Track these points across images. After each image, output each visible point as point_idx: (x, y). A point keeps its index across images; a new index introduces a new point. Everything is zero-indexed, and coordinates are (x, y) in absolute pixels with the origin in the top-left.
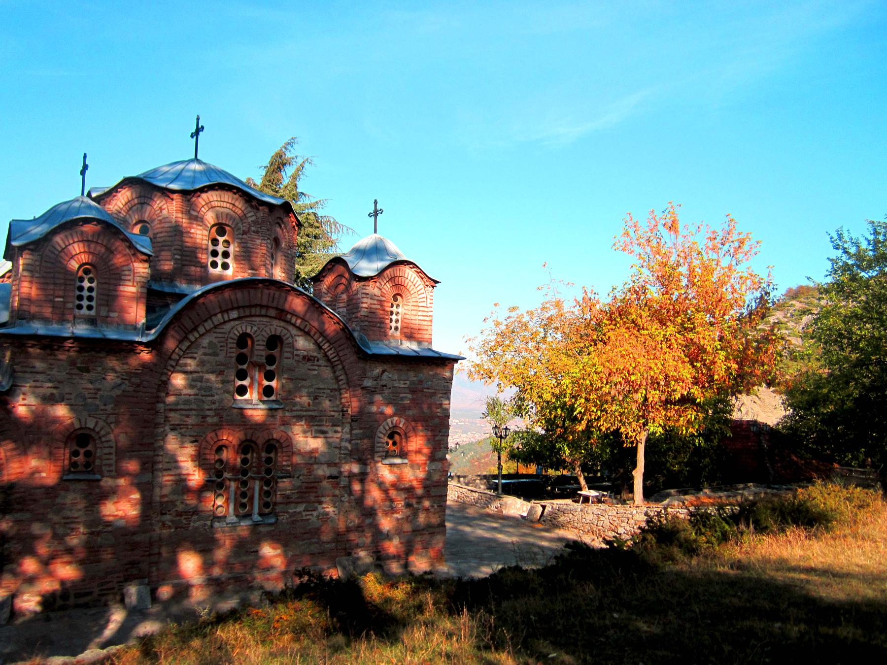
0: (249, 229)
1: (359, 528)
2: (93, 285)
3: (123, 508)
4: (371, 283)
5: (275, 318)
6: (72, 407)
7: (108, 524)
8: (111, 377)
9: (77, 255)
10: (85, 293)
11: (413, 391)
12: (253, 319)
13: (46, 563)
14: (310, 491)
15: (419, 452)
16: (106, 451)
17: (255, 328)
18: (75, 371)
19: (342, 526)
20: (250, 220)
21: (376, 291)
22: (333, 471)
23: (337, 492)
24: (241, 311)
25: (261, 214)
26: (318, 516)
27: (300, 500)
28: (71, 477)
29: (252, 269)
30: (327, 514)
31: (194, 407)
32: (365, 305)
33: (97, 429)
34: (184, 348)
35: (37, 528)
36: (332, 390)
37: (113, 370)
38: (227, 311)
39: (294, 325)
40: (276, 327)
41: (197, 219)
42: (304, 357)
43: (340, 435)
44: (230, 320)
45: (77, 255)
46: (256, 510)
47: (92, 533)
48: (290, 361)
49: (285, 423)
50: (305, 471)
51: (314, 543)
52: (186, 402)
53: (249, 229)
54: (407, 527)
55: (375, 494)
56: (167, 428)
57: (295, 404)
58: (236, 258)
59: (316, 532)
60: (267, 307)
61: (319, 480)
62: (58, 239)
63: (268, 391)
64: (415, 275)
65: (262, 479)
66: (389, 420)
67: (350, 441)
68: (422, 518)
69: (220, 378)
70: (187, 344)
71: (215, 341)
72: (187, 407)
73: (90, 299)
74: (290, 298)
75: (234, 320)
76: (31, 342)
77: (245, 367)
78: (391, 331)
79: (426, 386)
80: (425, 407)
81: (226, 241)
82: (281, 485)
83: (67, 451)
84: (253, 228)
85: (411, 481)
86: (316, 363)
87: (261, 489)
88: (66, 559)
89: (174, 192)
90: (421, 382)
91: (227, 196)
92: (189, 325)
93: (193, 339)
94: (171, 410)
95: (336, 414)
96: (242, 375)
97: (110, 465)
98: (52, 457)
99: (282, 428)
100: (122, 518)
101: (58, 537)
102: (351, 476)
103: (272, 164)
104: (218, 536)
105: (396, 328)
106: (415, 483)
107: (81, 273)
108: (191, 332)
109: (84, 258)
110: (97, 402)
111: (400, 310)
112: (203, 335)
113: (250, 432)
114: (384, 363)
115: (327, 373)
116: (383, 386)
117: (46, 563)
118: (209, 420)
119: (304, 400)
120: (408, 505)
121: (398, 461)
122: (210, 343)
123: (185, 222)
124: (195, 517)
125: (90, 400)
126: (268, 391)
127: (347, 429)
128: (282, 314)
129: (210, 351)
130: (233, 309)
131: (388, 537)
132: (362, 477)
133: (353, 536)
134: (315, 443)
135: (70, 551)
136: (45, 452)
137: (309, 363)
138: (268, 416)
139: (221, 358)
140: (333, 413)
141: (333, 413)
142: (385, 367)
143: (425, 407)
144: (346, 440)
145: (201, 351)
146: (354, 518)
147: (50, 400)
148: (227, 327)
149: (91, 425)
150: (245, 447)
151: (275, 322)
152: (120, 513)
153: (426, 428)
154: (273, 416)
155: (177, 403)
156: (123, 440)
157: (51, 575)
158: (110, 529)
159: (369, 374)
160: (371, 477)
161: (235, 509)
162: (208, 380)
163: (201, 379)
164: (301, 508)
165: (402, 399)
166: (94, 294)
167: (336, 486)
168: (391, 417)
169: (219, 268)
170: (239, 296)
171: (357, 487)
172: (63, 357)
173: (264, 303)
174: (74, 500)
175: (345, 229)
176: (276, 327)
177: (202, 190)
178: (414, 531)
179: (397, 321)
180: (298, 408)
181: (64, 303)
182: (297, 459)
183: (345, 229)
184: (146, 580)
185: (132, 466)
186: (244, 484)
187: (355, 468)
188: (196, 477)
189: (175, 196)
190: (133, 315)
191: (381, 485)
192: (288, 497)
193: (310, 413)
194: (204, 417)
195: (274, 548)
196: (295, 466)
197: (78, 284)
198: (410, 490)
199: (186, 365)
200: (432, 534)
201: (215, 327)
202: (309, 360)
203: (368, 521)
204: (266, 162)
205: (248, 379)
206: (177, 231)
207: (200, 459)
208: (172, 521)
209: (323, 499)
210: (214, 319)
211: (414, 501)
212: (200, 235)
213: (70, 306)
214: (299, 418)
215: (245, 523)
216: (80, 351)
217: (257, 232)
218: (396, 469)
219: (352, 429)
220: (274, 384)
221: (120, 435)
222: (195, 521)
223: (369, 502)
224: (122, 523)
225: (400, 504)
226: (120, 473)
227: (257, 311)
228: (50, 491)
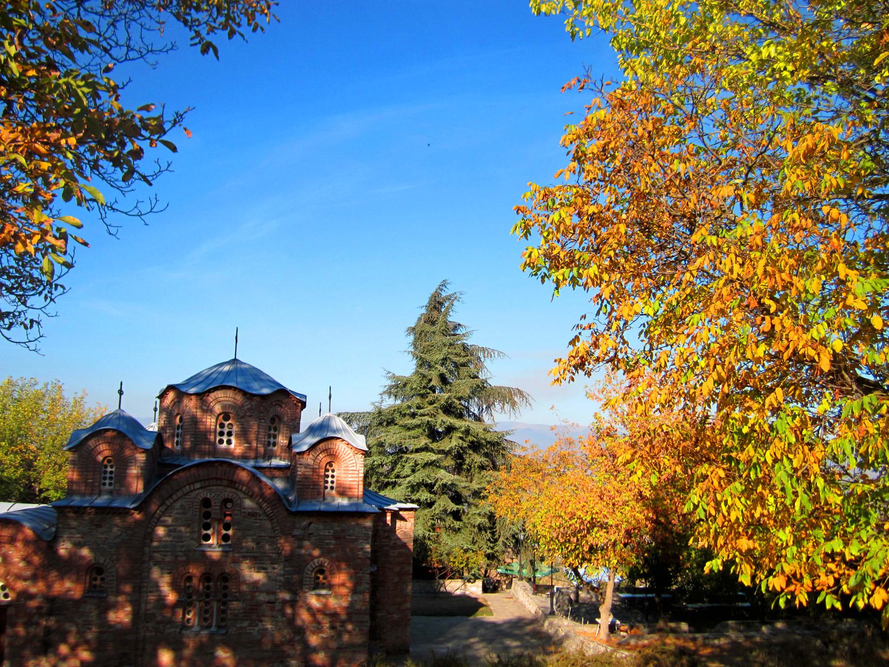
1: (291, 642)
2: (113, 469)
3: (121, 616)
4: (305, 456)
5: (227, 486)
6: (92, 550)
7: (111, 626)
8: (115, 529)
9: (104, 450)
10: (108, 475)
11: (336, 538)
13: (74, 648)
14: (254, 612)
15: (343, 585)
19: (278, 638)
20: (246, 408)
21: (310, 462)
22: (272, 598)
23: (275, 613)
25: (254, 403)
26: (258, 631)
28: (90, 594)
29: (247, 443)
30: (267, 629)
31: (170, 549)
32: (299, 473)
35: (67, 626)
37: (117, 526)
38: (193, 483)
39: (241, 490)
40: (228, 493)
41: (208, 410)
42: (249, 514)
43: (278, 569)
45: (104, 450)
46: (214, 624)
47: (100, 632)
49: (236, 562)
50: (249, 597)
52: (165, 547)
54: (333, 645)
55: (304, 616)
56: (151, 564)
57: (242, 548)
59: (259, 642)
60: (221, 479)
61: (260, 604)
62: (92, 443)
63: (226, 538)
64: (345, 446)
65: (218, 601)
66: (316, 560)
67: (283, 575)
68: (346, 637)
69: (188, 530)
70: (165, 507)
73: (111, 478)
74: (238, 472)
76: (68, 510)
77: (209, 521)
78: (327, 491)
80: (348, 550)
81: (230, 424)
82: (231, 606)
83: (88, 577)
85: (335, 608)
87: (218, 608)
88: (86, 647)
89: (191, 395)
91: (230, 393)
94: (154, 552)
96: (207, 527)
98: (77, 581)
99: (232, 565)
100: (120, 623)
101: (80, 633)
102: (284, 602)
103: (430, 304)
104: (185, 640)
105: (332, 488)
106: (338, 610)
107: (105, 462)
109: (107, 453)
110: (105, 546)
111: (334, 474)
115: (268, 525)
117: (74, 648)
118: (180, 559)
119: (250, 544)
120: (332, 628)
121: (324, 592)
122: (182, 506)
123: (199, 414)
124: (168, 626)
126: (226, 538)
127: (281, 567)
128: (233, 483)
131: (315, 650)
132: (293, 603)
133: (285, 648)
134: (258, 576)
135: (87, 642)
136: (74, 577)
138: (222, 556)
142: (312, 520)
143: (348, 550)
144: (281, 575)
145: (175, 512)
146: (287, 633)
147: (79, 545)
148: (193, 494)
149: (101, 561)
150: (206, 577)
151: (229, 489)
152: (118, 620)
153: (349, 566)
154: (226, 556)
155: (158, 547)
156: (122, 571)
157: (76, 656)
158: (111, 630)
160: (300, 603)
161: (199, 621)
162: (180, 531)
163: (174, 531)
164: (245, 624)
165: (327, 544)
166: (113, 475)
167: (273, 609)
168: (317, 558)
169: (225, 444)
170: (202, 472)
171: (289, 611)
172: (87, 518)
174: (92, 610)
175: (496, 353)
176: (228, 493)
177: (210, 391)
178: (338, 648)
179: (332, 482)
180: (245, 550)
181: (93, 483)
182: (244, 588)
183: (496, 353)
185: (128, 588)
186: (207, 603)
187: (286, 596)
188: (171, 597)
189: (193, 397)
190: (135, 488)
191: (310, 609)
192: (236, 615)
194: (177, 556)
195: (225, 652)
196: (242, 593)
197: (104, 469)
198: (334, 615)
199: (165, 521)
200: (354, 652)
201: (185, 495)
202: (253, 515)
203: (297, 638)
204: (426, 302)
205: (211, 530)
206: (195, 421)
207: (174, 585)
209: (263, 618)
210: (184, 489)
211: (338, 624)
212: (210, 422)
213: (97, 484)
214: (245, 558)
215: (205, 632)
216: (96, 514)
217: (251, 416)
218: (321, 598)
220: (230, 532)
221: (122, 568)
223: (299, 622)
224: (119, 626)
225: (326, 625)
226: (119, 593)
228: (77, 603)
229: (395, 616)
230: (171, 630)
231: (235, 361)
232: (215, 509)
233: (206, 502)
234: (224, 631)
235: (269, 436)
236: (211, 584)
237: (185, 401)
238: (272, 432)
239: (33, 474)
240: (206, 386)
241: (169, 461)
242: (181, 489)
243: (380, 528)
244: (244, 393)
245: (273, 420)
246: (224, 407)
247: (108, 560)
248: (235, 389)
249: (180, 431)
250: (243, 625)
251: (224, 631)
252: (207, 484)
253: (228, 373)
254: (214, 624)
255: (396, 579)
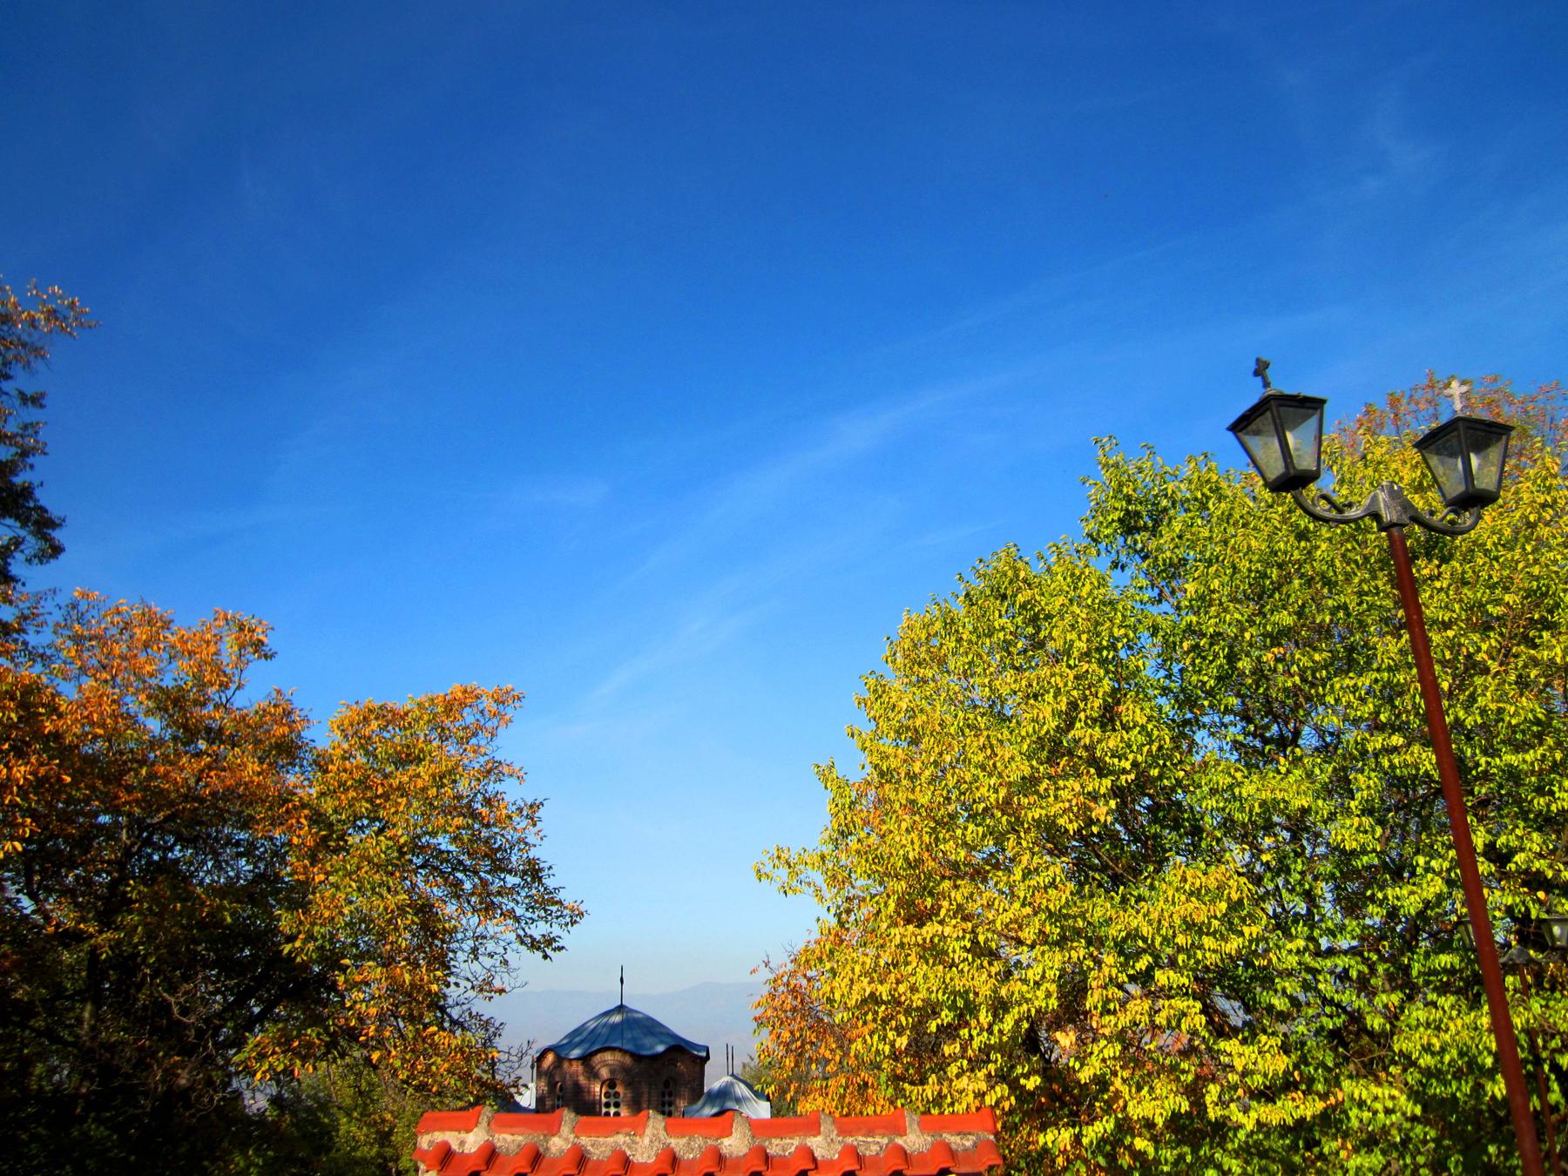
41: (593, 1074)
58: (629, 1106)
91: (618, 1056)
123: (582, 1080)
231: (621, 1008)
237: (566, 1065)
239: (389, 1152)
240: (590, 1041)
244: (632, 1055)
245: (666, 1084)
246: (612, 1072)
248: (621, 1050)
253: (614, 1027)
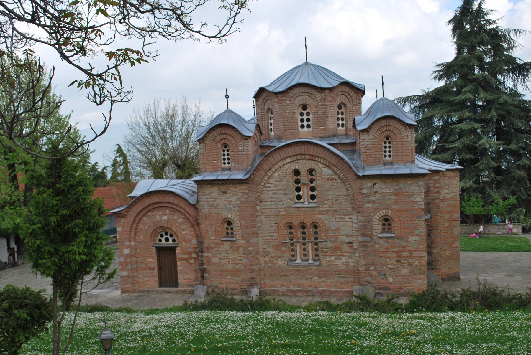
0: (318, 104)
11: (396, 194)
12: (299, 161)
16: (237, 228)
17: (300, 166)
18: (221, 193)
20: (318, 99)
24: (292, 158)
26: (343, 263)
27: (332, 254)
31: (274, 207)
33: (232, 218)
34: (266, 179)
36: (345, 196)
44: (287, 163)
46: (311, 258)
48: (320, 182)
51: (342, 277)
53: (318, 104)
71: (281, 174)
72: (271, 207)
75: (289, 163)
77: (299, 185)
79: (405, 190)
84: (320, 104)
86: (335, 181)
87: (313, 247)
90: (401, 188)
92: (267, 168)
93: (270, 175)
95: (349, 209)
97: (239, 234)
108: (268, 171)
110: (231, 206)
112: (275, 172)
113: (303, 218)
114: (374, 179)
116: (375, 192)
122: (279, 175)
124: (279, 259)
125: (228, 206)
129: (279, 180)
130: (287, 157)
137: (331, 182)
139: (285, 182)
140: (347, 208)
141: (347, 208)
142: (376, 181)
145: (274, 180)
148: (286, 167)
149: (229, 216)
151: (310, 162)
159: (365, 186)
164: (333, 258)
173: (303, 153)
184: (259, 287)
193: (334, 209)
194: (279, 212)
201: (280, 167)
202: (331, 180)
208: (269, 261)
219: (358, 217)
222: (279, 261)
227: (300, 157)
229: (448, 252)
230: (281, 263)
232: (304, 178)
233: (297, 172)
234: (318, 263)
235: (338, 119)
236: (306, 230)
238: (340, 116)
241: (267, 144)
242: (277, 163)
243: (431, 185)
245: (340, 107)
247: (233, 216)
249: (272, 121)
250: (331, 259)
251: (318, 263)
252: (295, 159)
254: (311, 258)
255: (447, 224)
